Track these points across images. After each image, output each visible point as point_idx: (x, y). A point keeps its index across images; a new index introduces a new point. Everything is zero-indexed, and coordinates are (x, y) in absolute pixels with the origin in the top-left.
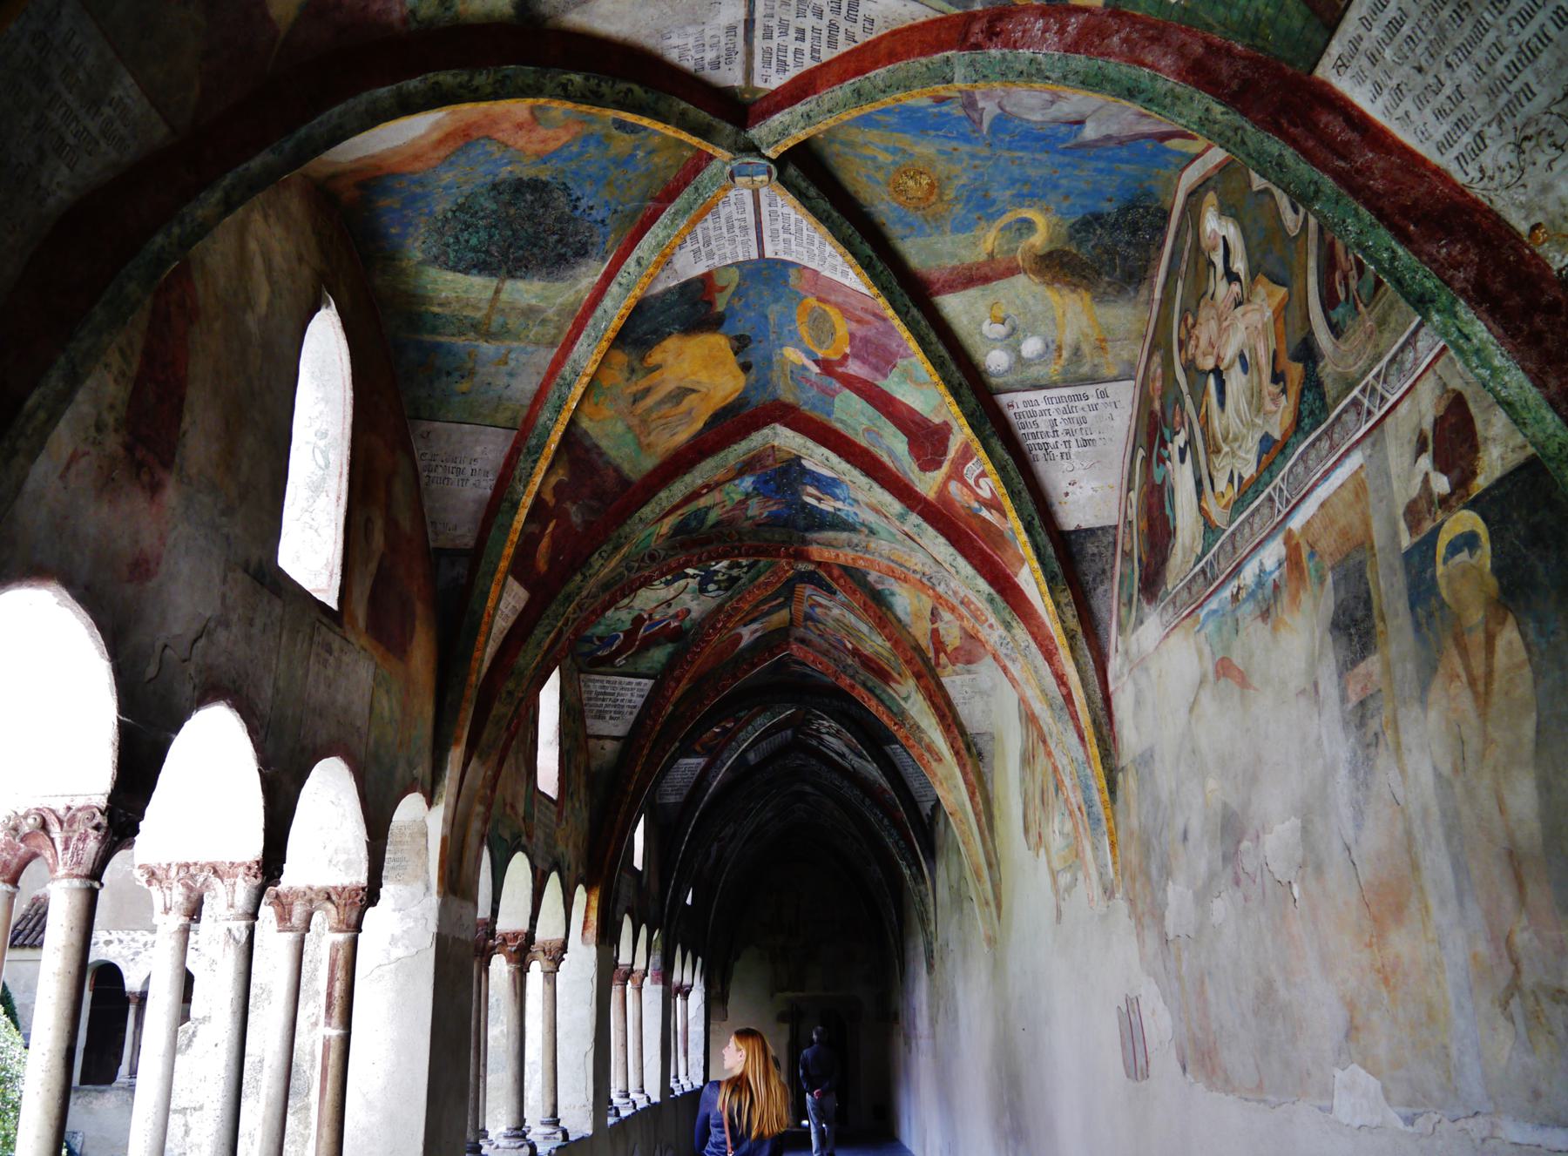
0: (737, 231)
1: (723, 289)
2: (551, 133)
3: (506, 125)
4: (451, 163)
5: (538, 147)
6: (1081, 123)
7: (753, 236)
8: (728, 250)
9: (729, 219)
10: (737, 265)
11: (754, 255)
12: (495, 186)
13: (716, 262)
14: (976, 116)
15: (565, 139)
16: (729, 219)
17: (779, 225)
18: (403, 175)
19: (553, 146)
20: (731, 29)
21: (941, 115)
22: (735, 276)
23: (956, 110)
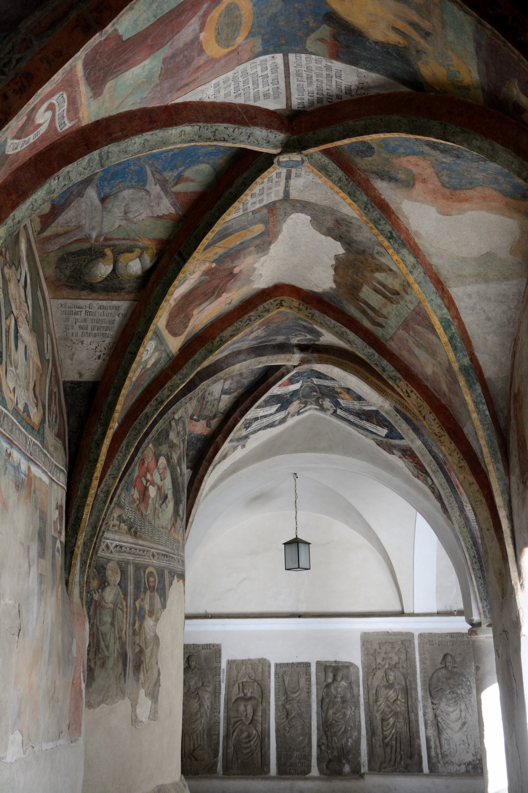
0: (304, 74)
1: (322, 40)
2: (411, 167)
3: (430, 186)
4: (471, 183)
5: (422, 163)
6: (103, 200)
7: (292, 69)
8: (313, 64)
9: (310, 83)
10: (306, 52)
11: (292, 57)
12: (458, 157)
13: (324, 62)
14: (157, 176)
15: (405, 159)
16: (310, 83)
17: (271, 77)
18: (500, 191)
19: (413, 159)
20: (298, 176)
21: (175, 167)
22: (310, 43)
23: (170, 175)
